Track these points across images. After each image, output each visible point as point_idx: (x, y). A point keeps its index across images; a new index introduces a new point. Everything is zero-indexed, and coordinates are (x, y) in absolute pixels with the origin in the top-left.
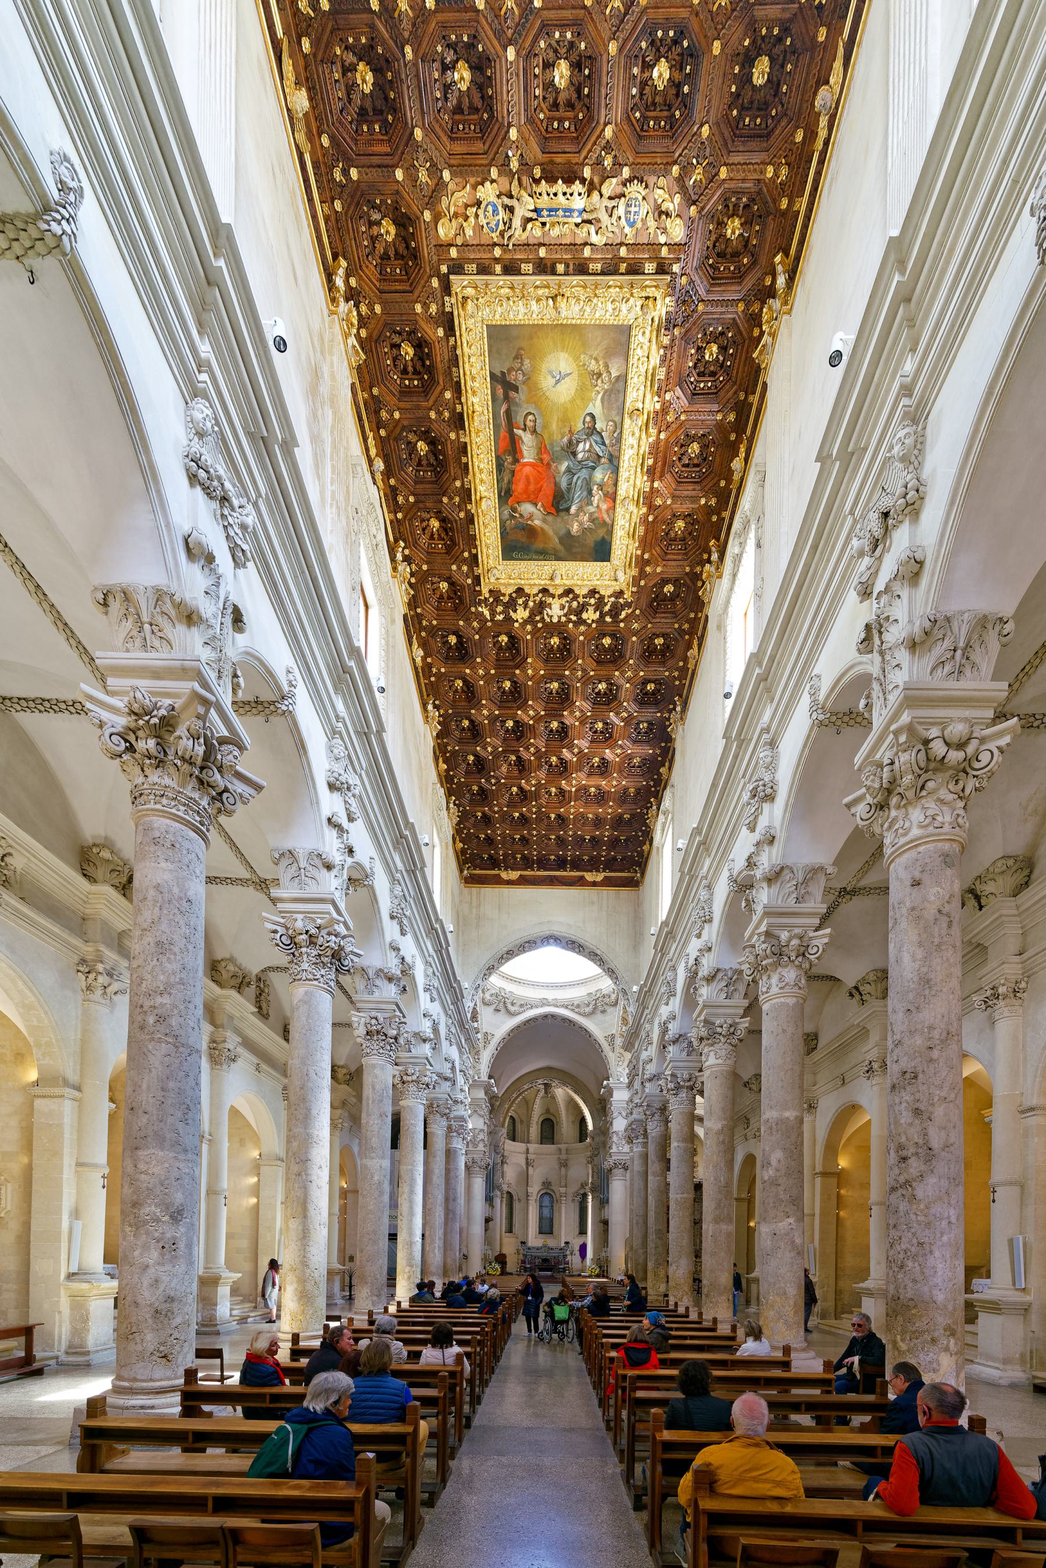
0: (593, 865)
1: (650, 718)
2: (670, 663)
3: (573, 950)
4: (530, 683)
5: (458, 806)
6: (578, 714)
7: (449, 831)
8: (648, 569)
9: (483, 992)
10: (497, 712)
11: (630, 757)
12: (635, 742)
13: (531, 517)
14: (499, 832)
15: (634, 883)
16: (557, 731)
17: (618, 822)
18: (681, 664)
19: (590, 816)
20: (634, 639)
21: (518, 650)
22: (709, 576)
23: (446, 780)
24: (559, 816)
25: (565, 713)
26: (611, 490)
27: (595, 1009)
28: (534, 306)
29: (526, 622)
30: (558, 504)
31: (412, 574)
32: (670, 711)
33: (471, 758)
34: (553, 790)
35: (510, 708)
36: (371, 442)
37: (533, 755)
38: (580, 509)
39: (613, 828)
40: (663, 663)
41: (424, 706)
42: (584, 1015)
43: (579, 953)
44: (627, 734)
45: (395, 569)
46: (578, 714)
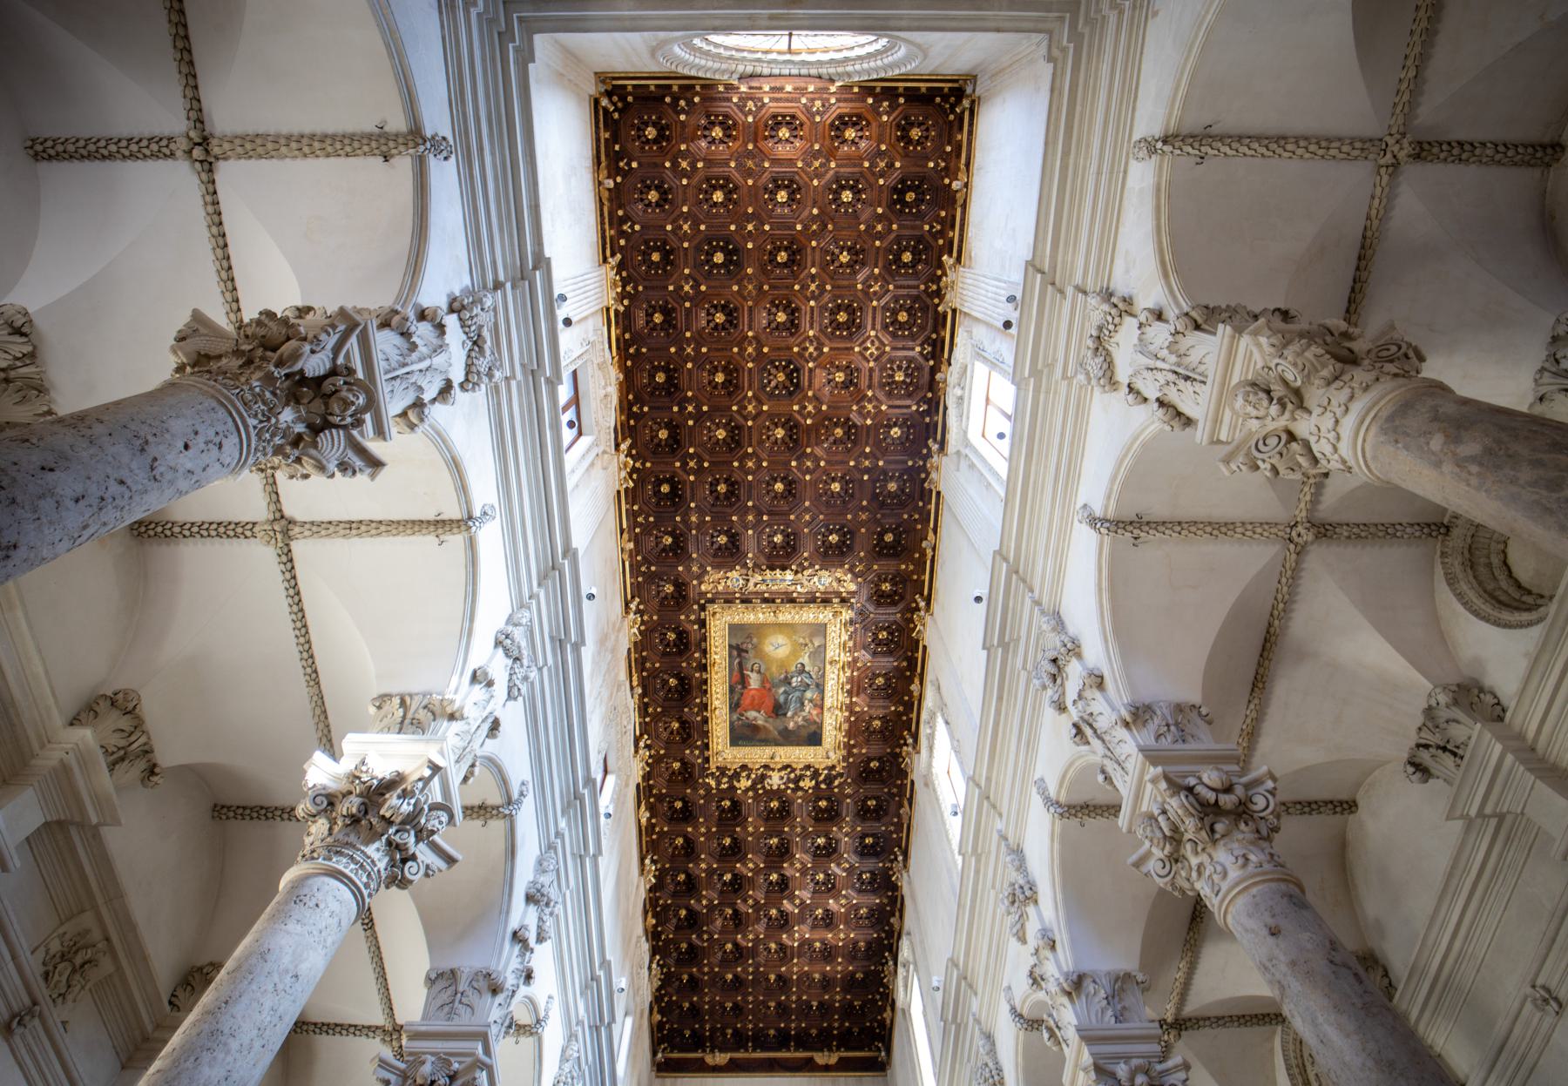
0: (824, 1041)
2: (886, 819)
5: (662, 967)
7: (647, 996)
8: (855, 751)
11: (857, 908)
12: (860, 891)
13: (755, 719)
17: (850, 983)
19: (817, 976)
21: (740, 812)
22: (908, 754)
23: (653, 935)
24: (780, 977)
26: (819, 703)
28: (761, 615)
29: (747, 790)
30: (778, 710)
31: (650, 757)
33: (683, 913)
34: (773, 946)
36: (635, 678)
38: (795, 714)
39: (845, 990)
40: (878, 819)
41: (642, 860)
45: (636, 752)
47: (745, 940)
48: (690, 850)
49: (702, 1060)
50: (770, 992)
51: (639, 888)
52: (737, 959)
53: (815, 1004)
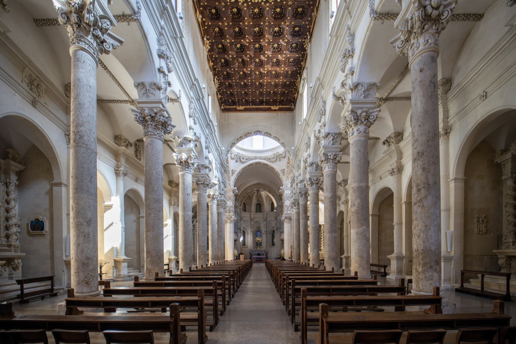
0: (275, 103)
1: (297, 42)
2: (305, 18)
3: (267, 136)
4: (246, 28)
5: (218, 80)
6: (267, 40)
7: (215, 89)
9: (231, 154)
10: (233, 41)
12: (291, 52)
14: (235, 90)
15: (291, 110)
16: (258, 48)
17: (284, 85)
18: (309, 19)
19: (273, 83)
20: (290, 8)
21: (241, 14)
23: (213, 69)
24: (260, 83)
25: (261, 40)
27: (276, 160)
32: (305, 39)
33: (223, 60)
34: (257, 73)
35: (239, 39)
37: (249, 58)
39: (282, 88)
41: (203, 38)
42: (272, 162)
44: (287, 48)
46: (267, 40)
47: (247, 71)
48: (222, 33)
49: (236, 108)
50: (256, 88)
51: (204, 51)
52: (244, 78)
53: (272, 92)
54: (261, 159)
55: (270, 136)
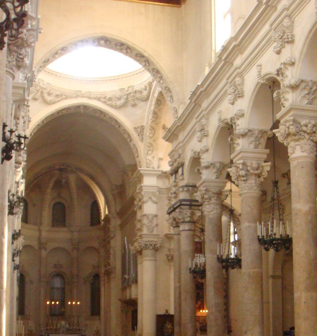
3: (121, 50)
43: (126, 53)
54: (90, 98)
55: (127, 52)
